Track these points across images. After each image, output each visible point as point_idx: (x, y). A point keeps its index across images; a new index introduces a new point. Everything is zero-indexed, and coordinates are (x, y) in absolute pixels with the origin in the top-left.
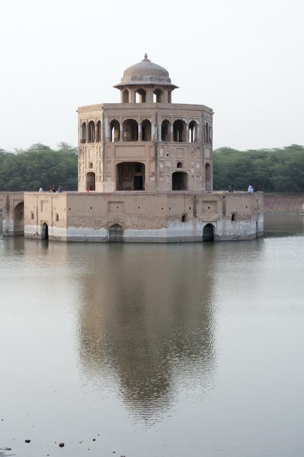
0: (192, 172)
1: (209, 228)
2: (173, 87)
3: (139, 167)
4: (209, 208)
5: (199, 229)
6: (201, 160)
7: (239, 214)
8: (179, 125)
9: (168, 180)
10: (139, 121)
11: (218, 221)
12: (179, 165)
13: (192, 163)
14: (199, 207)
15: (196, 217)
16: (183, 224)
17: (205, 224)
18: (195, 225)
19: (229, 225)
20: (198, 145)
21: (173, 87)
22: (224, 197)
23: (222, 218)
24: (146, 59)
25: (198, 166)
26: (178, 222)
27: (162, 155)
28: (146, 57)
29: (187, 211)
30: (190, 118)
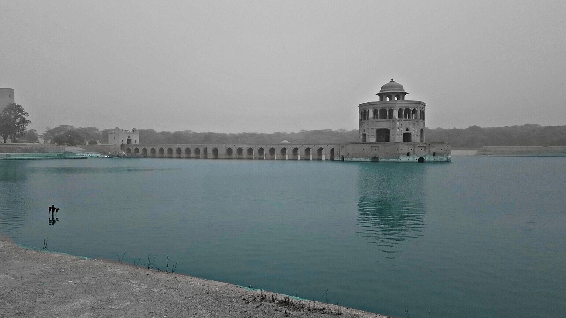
2: (406, 93)
3: (387, 131)
5: (417, 159)
8: (408, 111)
10: (387, 109)
12: (407, 130)
14: (416, 150)
19: (432, 159)
21: (406, 93)
26: (405, 156)
29: (410, 151)
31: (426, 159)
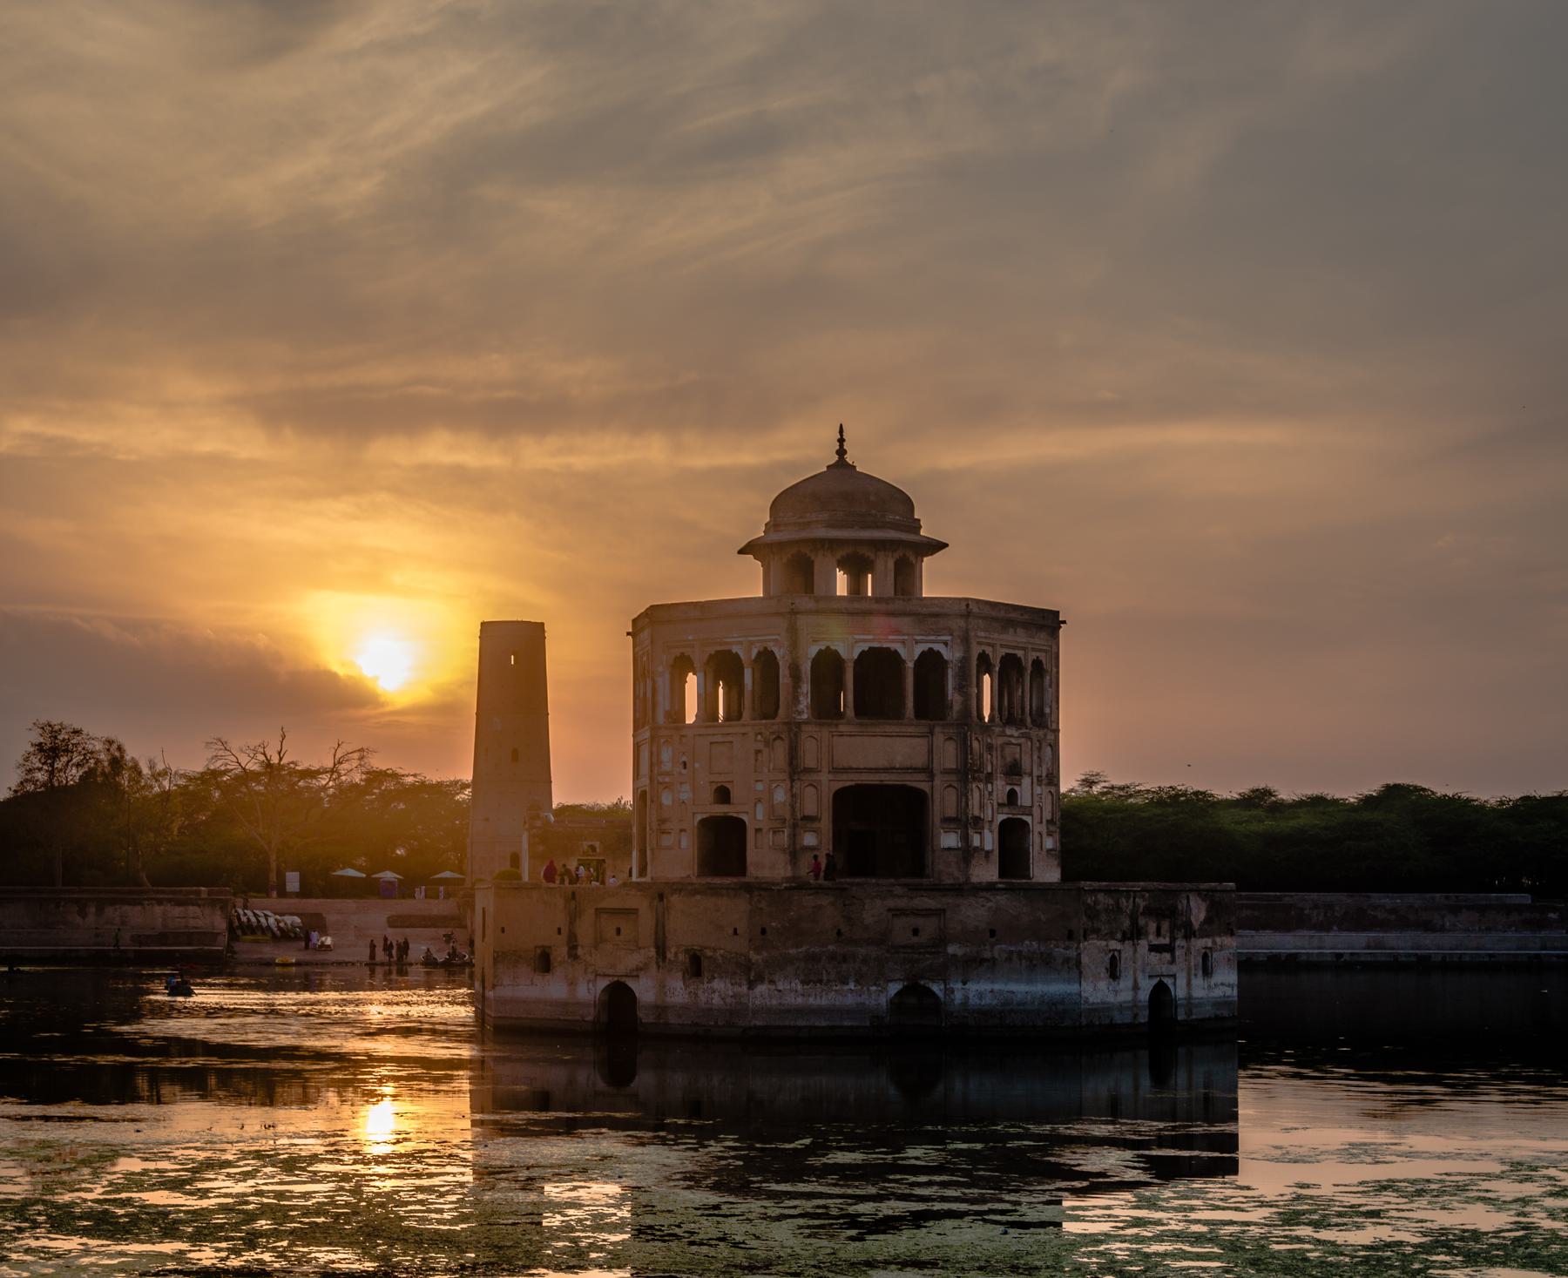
0: (760, 816)
1: (619, 996)
4: (618, 931)
6: (785, 776)
7: (709, 953)
9: (684, 844)
11: (641, 974)
12: (723, 795)
13: (760, 787)
15: (576, 957)
16: (538, 978)
17: (603, 983)
18: (572, 983)
19: (678, 991)
20: (775, 728)
22: (661, 897)
23: (654, 967)
24: (842, 464)
25: (780, 796)
27: (667, 767)
28: (841, 452)
30: (752, 643)
31: (644, 990)
